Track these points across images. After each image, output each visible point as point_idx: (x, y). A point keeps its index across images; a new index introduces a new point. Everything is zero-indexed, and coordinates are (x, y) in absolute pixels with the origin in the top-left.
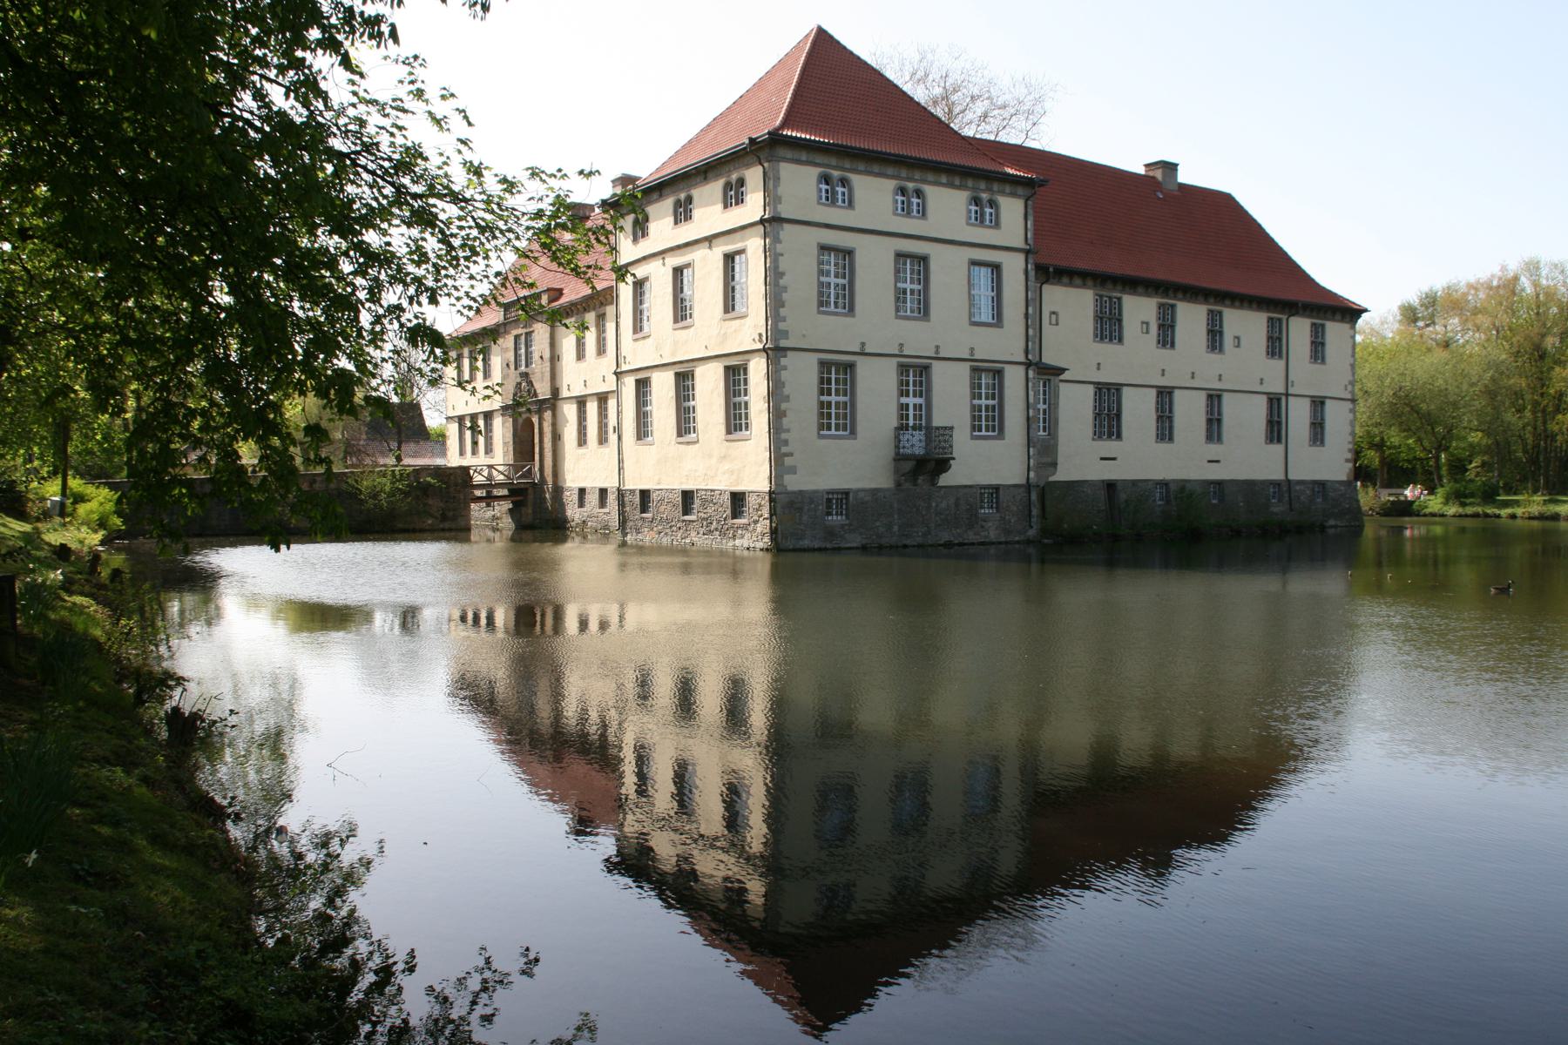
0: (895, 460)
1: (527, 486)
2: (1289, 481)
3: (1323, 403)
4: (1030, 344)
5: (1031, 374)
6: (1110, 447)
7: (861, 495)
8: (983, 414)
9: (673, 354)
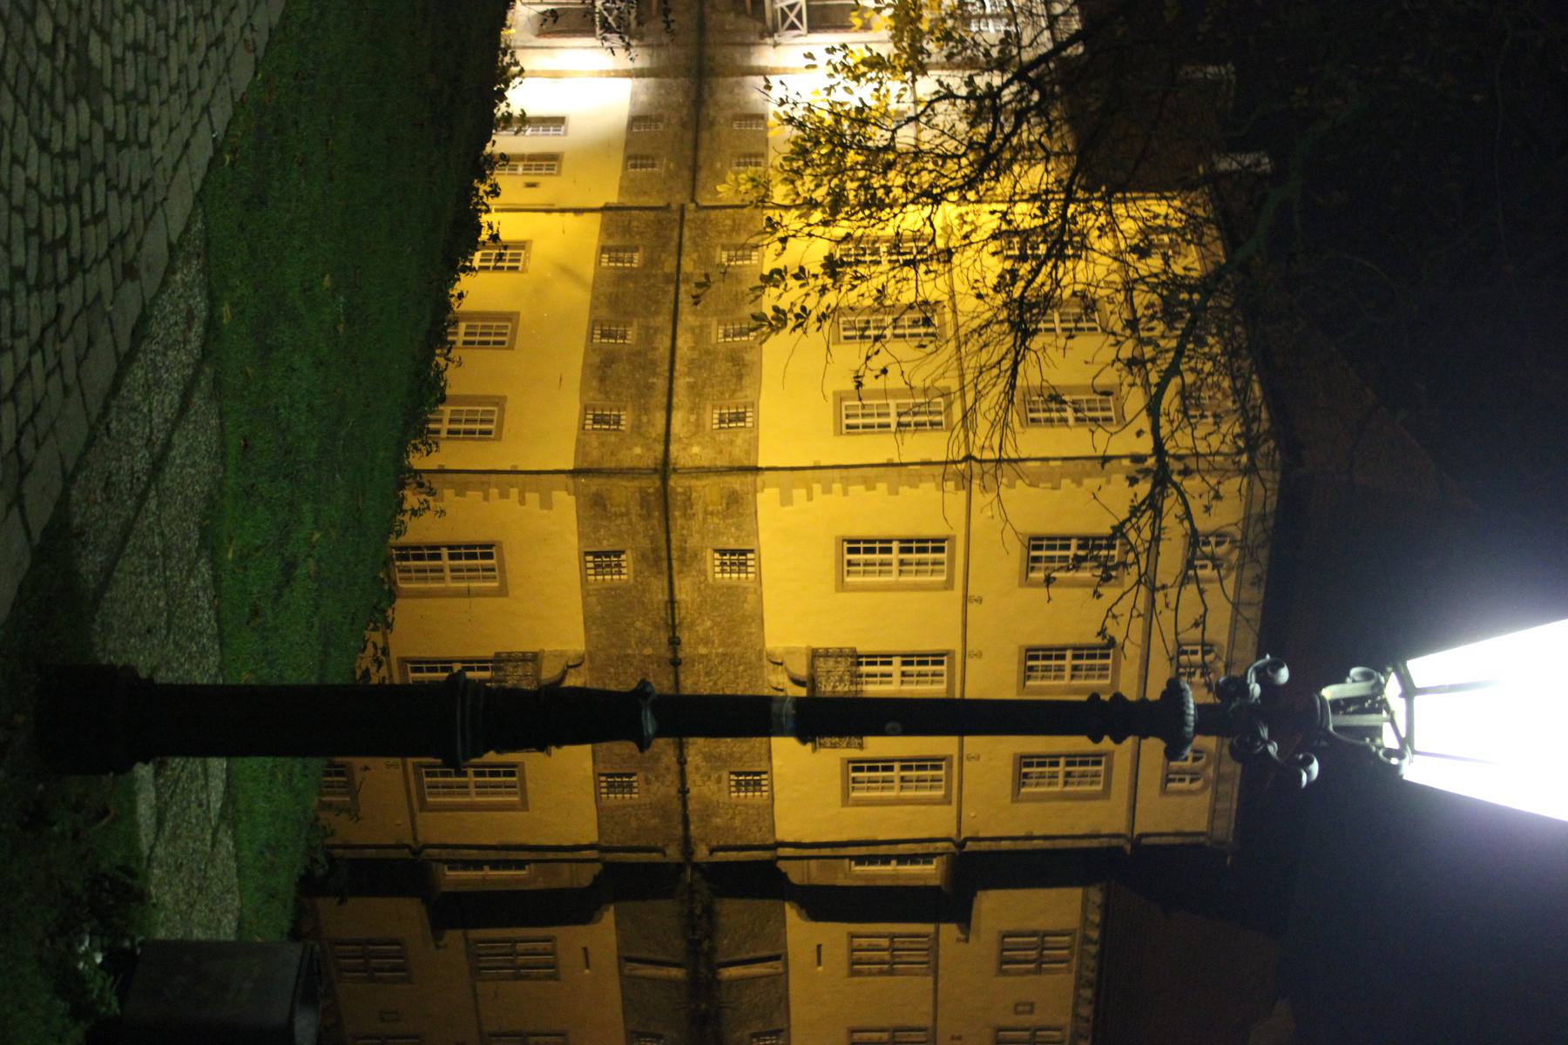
7: (751, 598)
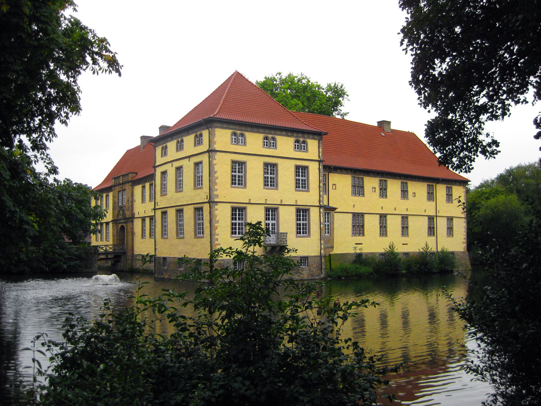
1: (121, 254)
3: (452, 219)
4: (321, 198)
5: (322, 210)
6: (359, 239)
8: (302, 227)
9: (176, 203)
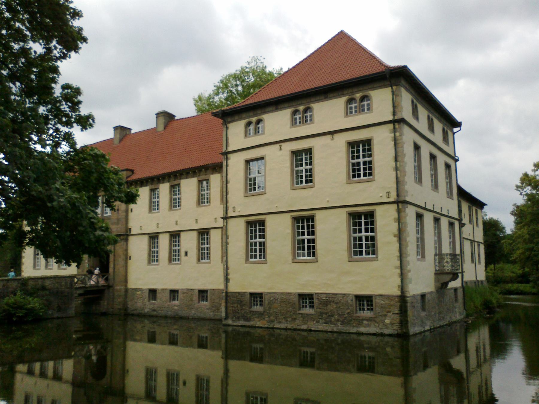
0: (435, 274)
2: (478, 281)
